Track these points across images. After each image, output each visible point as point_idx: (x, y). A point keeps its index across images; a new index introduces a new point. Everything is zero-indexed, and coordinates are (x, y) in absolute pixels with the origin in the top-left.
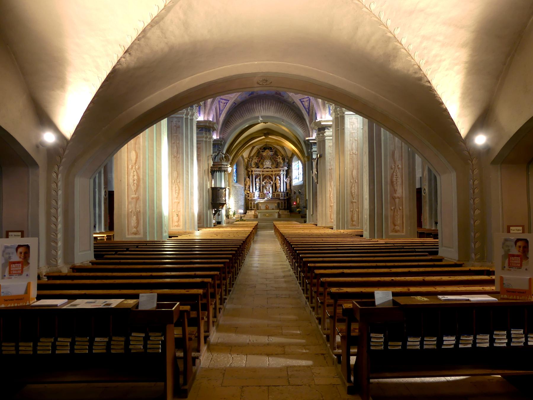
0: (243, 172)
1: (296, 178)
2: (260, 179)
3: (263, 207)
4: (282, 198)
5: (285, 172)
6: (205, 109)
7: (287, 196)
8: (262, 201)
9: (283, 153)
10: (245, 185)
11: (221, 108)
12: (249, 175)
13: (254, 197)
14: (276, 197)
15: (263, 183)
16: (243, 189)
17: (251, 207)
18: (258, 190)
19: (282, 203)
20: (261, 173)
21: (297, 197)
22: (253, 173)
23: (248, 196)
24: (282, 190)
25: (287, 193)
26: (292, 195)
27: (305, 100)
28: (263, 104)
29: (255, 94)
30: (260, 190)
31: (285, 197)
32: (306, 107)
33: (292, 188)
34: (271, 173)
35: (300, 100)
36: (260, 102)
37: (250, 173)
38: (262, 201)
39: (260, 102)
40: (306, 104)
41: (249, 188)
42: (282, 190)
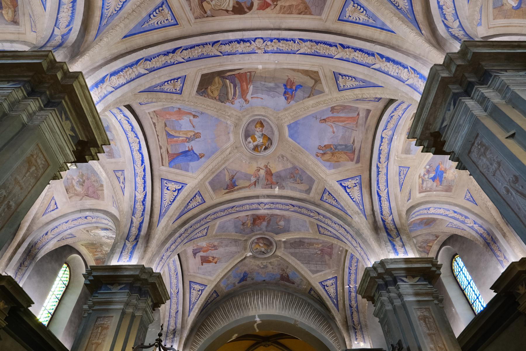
6: (145, 251)
11: (193, 300)
27: (329, 283)
28: (262, 297)
29: (249, 281)
32: (333, 295)
35: (321, 283)
36: (257, 294)
39: (257, 294)
40: (332, 290)
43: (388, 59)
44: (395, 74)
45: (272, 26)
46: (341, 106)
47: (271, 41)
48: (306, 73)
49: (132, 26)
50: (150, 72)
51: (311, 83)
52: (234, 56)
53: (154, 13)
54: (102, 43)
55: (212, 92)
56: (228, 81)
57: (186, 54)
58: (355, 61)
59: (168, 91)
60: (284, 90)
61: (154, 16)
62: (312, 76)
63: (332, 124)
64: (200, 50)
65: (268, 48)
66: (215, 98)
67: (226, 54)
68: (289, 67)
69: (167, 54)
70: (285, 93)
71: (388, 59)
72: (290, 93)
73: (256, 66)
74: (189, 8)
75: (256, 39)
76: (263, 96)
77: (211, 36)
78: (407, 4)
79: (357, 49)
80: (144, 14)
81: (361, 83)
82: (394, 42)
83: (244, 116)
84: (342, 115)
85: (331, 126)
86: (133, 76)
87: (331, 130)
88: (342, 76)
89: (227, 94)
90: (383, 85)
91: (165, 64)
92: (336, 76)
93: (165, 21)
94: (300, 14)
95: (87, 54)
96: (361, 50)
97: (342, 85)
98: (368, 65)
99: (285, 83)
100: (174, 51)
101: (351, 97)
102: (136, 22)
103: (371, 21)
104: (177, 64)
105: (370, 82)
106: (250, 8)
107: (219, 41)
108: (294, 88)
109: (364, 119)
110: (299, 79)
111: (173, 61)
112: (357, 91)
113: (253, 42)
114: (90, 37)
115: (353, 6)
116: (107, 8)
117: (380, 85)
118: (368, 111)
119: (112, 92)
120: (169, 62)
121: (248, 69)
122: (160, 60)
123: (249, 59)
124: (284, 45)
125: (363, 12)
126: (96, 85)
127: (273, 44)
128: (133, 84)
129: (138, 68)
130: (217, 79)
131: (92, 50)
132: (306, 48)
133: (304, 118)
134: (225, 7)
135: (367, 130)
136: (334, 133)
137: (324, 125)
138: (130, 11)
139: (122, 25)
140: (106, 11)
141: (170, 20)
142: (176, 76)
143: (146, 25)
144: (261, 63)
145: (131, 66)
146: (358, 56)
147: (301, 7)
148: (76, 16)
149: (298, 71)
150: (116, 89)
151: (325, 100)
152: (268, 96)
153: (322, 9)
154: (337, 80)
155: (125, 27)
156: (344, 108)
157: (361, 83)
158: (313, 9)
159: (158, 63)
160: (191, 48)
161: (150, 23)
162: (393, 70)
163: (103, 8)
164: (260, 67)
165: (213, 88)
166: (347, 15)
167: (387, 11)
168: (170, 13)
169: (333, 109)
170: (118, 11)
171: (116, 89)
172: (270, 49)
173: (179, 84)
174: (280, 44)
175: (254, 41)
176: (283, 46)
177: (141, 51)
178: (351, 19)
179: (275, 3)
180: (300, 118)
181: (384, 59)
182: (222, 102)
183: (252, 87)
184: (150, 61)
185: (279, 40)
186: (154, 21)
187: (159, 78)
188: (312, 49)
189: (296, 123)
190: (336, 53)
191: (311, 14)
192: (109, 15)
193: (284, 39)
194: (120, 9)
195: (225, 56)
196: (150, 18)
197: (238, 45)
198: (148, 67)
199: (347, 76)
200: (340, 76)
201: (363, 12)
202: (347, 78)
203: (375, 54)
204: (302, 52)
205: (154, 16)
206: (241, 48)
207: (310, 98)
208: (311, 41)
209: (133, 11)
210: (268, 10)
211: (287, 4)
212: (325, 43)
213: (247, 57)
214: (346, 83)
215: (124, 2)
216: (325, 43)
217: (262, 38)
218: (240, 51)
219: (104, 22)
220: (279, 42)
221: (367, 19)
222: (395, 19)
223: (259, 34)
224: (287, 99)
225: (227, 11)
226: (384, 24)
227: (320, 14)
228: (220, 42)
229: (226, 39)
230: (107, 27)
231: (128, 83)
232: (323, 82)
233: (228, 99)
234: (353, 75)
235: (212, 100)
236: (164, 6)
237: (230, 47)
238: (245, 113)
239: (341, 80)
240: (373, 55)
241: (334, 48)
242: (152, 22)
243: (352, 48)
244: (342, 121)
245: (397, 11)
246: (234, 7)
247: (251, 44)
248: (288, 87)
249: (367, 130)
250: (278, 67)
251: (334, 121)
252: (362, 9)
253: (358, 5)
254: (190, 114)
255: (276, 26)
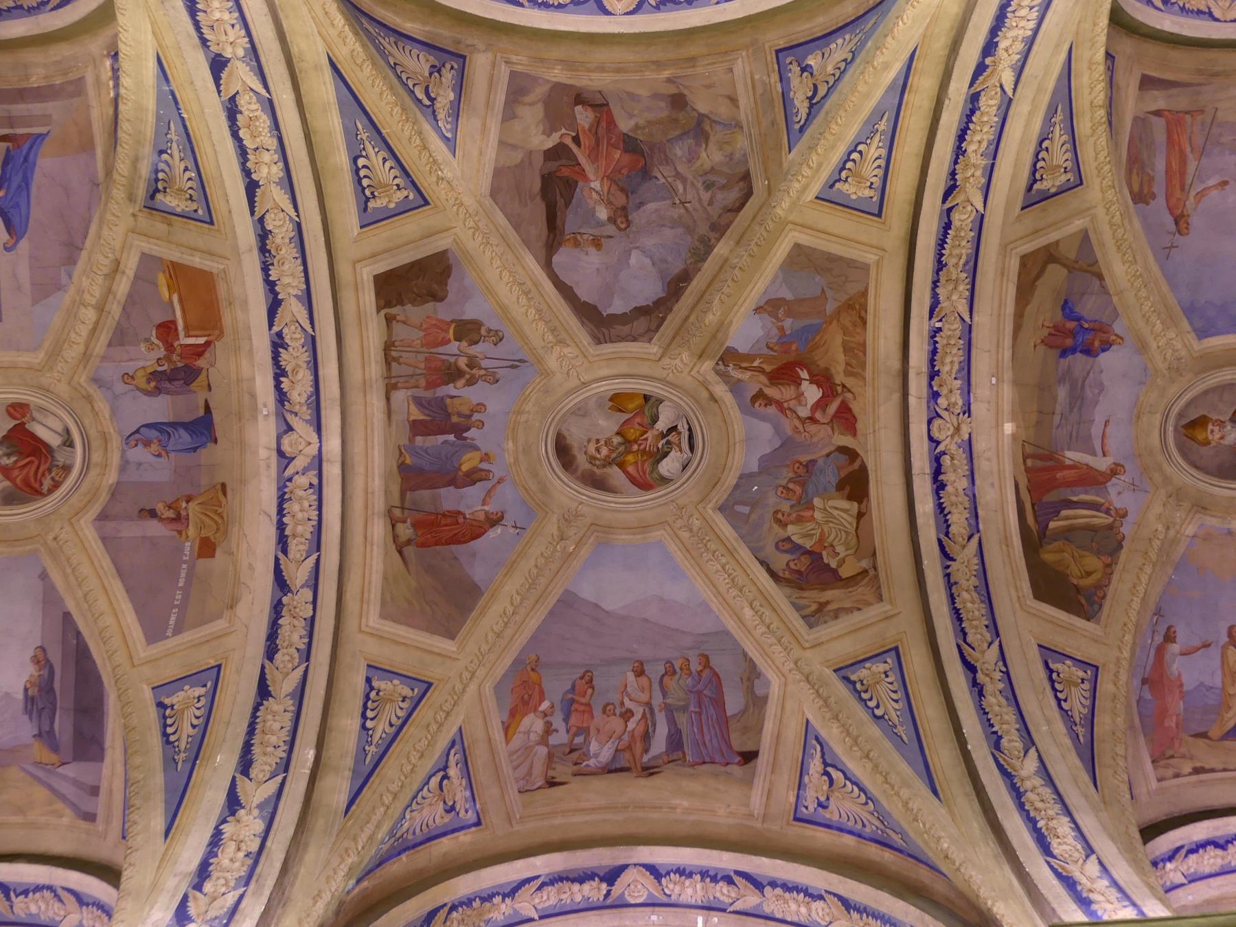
43: (990, 48)
44: (1034, 14)
45: (896, 397)
46: (1129, 172)
47: (935, 395)
48: (1025, 291)
49: (904, 767)
50: (1034, 744)
51: (1055, 275)
52: (981, 501)
53: (872, 704)
54: (957, 855)
55: (1089, 574)
56: (1052, 525)
57: (978, 634)
58: (993, 147)
59: (1087, 703)
60: (1078, 355)
61: (878, 706)
62: (1035, 273)
63: (1193, 193)
64: (965, 595)
65: (955, 404)
66: (1108, 566)
67: (973, 522)
68: (1007, 342)
69: (978, 690)
70: (1089, 352)
71: (990, 48)
72: (1089, 336)
73: (1007, 442)
74: (856, 613)
75: (931, 439)
76: (1099, 419)
77: (925, 562)
78: (840, 41)
79: (959, 147)
80: (874, 730)
81: (1059, 117)
82: (939, 46)
83: (1167, 480)
84: (1160, 165)
85: (1201, 195)
86: (1047, 792)
87: (1214, 193)
88: (1035, 181)
89: (1093, 529)
90: (1066, 47)
91: (1007, 699)
92: (1034, 198)
93: (889, 680)
94: (865, 323)
95: (989, 903)
96: (961, 137)
97: (1064, 178)
98: (1004, 107)
99: (1057, 352)
100: (970, 668)
101: (1103, 141)
102: (896, 757)
103: (883, 126)
104: (1005, 665)
105: (1055, 92)
106: (851, 454)
107: (940, 541)
108: (1071, 325)
109: (1174, 91)
110: (1044, 310)
111: (998, 675)
112: (1083, 126)
113: (941, 448)
114: (939, 887)
115: (846, 181)
116: (859, 826)
117: (1063, 56)
118: (1147, 83)
119: (1101, 863)
120: (1001, 686)
121: (1015, 464)
122: (997, 708)
123: (989, 460)
124: (948, 360)
125: (860, 152)
126: (1085, 903)
127: (944, 391)
128: (1074, 798)
129: (1024, 773)
130: (1048, 556)
131: (975, 888)
132: (954, 297)
133: (1174, 287)
134: (849, 519)
135: (1215, 75)
136: (1225, 183)
137: (1196, 221)
138: (869, 766)
139: (905, 793)
140: (868, 830)
141: (887, 667)
142: (1042, 674)
143: (900, 730)
144: (998, 425)
145: (1017, 794)
146: (976, 145)
147: (846, 320)
148: (883, 909)
149: (1019, 316)
150: (1093, 852)
151: (1111, 224)
152: (1097, 403)
153: (851, 263)
154: (1046, 196)
155: (909, 787)
156: (1135, 163)
157: (1059, 117)
158: (853, 289)
159: (1006, 717)
160: (960, 620)
161: (896, 720)
162: (1022, 23)
163: (860, 836)
164: (1009, 428)
165: (1074, 570)
166: (868, 193)
167: (861, 88)
168: (868, 665)
169: (1141, 198)
170: (868, 798)
171: (1090, 850)
172: (958, 399)
173: (1064, 669)
174: (946, 372)
175: (938, 443)
176: (949, 364)
177: (974, 756)
178: (877, 182)
179: (839, 389)
180: (1172, 300)
181: (988, 61)
182: (1120, 546)
183: (1069, 454)
184: (1001, 737)
185: (933, 375)
186: (892, 709)
187: (1049, 722)
188: (957, 280)
189: (1190, 311)
190: (969, 208)
191: (864, 294)
192: (877, 823)
193: (932, 362)
194: (861, 789)
195: (981, 526)
196: (882, 717)
197: (949, 488)
198: (1019, 745)
199: (1035, 165)
200: (1036, 187)
201: (860, 152)
202: (1039, 165)
203: (972, 91)
204: (967, 308)
205: (878, 706)
206: (956, 481)
207: (1105, 272)
208: (935, 284)
209: (867, 756)
210: (855, 407)
211: (841, 357)
212: (942, 243)
213: (982, 465)
214: (1060, 167)
215: (846, 778)
216: (942, 243)
217: (930, 422)
218: (964, 483)
219: (897, 839)
220: (938, 373)
221: (877, 138)
222: (879, 60)
223: (918, 429)
224: (1106, 346)
225: (860, 515)
226: (891, 87)
227: (865, 268)
228: (942, 536)
229: (932, 522)
230: (912, 835)
231: (1069, 813)
232: (1054, 236)
233: (1110, 527)
234: (1032, 148)
235: (1115, 577)
236: (853, 677)
237: (953, 510)
238: (1157, 477)
239: (1047, 184)
240: (974, 98)
241: (956, 217)
242: (893, 715)
243: (956, 162)
244: (1183, 162)
245: (858, 61)
246: (850, 498)
247: (945, 453)
248: (1069, 342)
249: (1215, 75)
250: (1008, 375)
251: (1182, 189)
252: (855, 156)
253: (843, 168)
254: (1160, 651)
255: (896, 384)
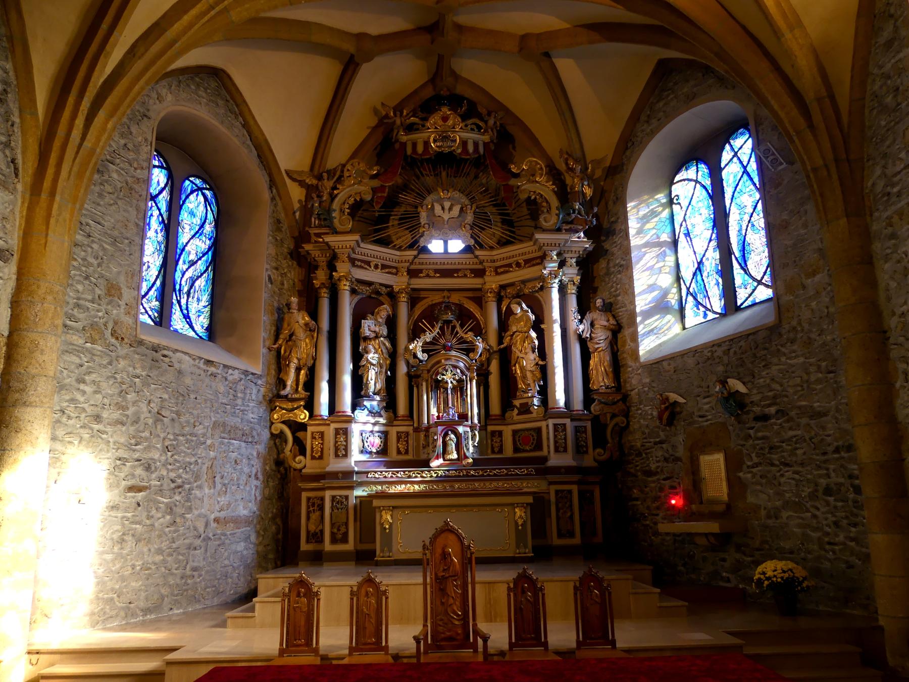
0: (263, 261)
1: (661, 307)
2: (391, 323)
3: (406, 535)
4: (565, 460)
5: (571, 273)
7: (600, 440)
8: (408, 483)
9: (552, 139)
10: (280, 362)
12: (312, 289)
13: (343, 451)
14: (511, 451)
15: (416, 346)
16: (256, 392)
17: (316, 537)
18: (373, 403)
19: (563, 497)
20: (399, 282)
21: (701, 444)
22: (343, 268)
23: (300, 447)
24: (560, 396)
25: (598, 424)
26: (636, 439)
30: (390, 404)
31: (580, 450)
33: (635, 381)
34: (472, 282)
37: (321, 276)
38: (408, 483)
41: (310, 386)
42: (560, 396)
